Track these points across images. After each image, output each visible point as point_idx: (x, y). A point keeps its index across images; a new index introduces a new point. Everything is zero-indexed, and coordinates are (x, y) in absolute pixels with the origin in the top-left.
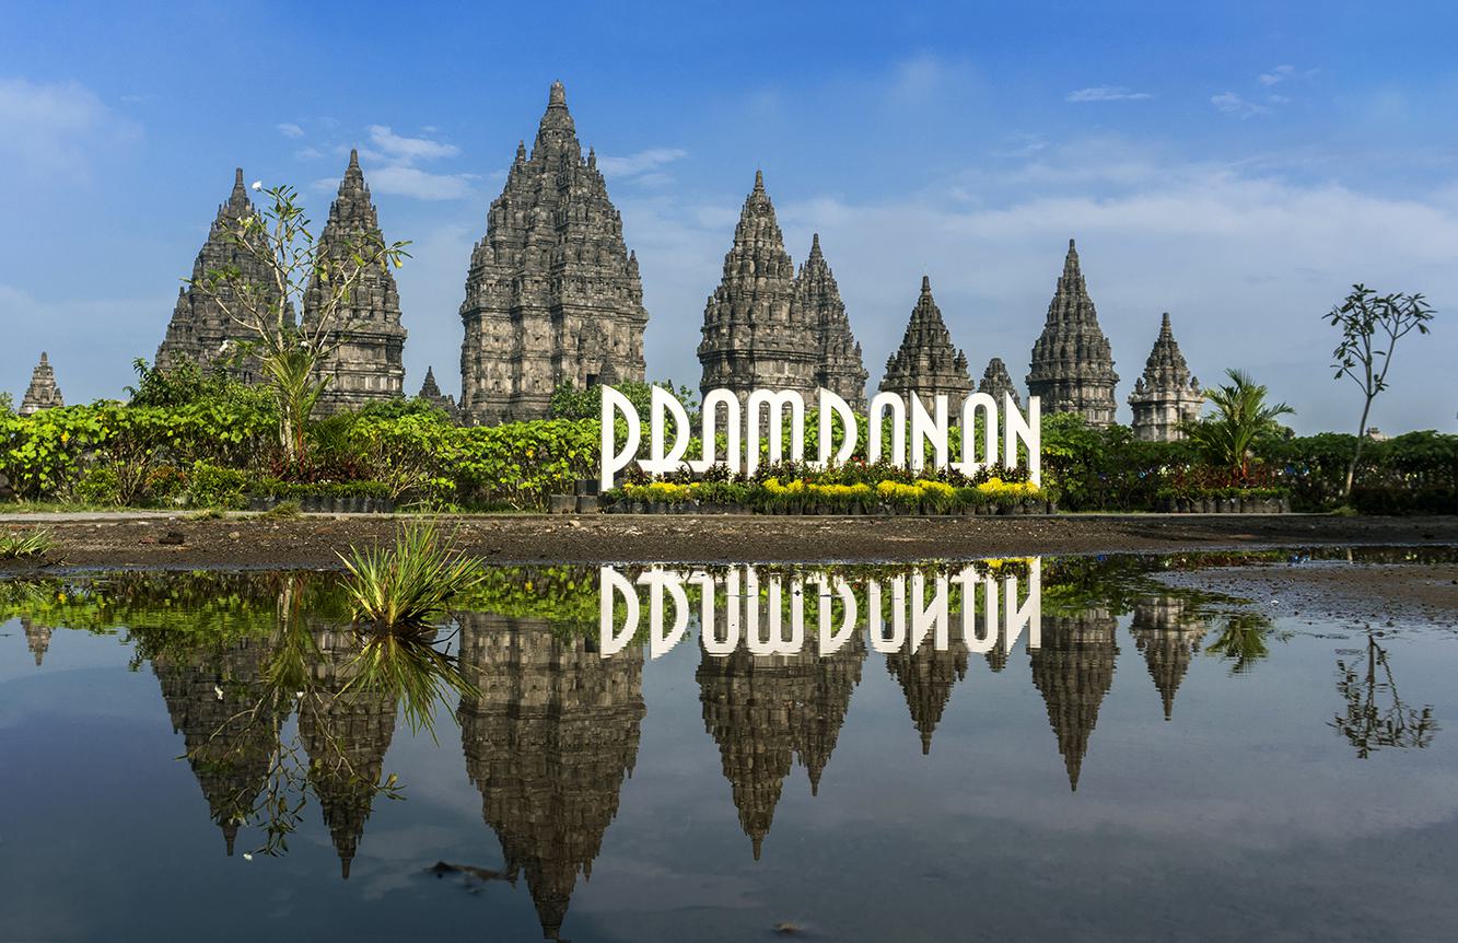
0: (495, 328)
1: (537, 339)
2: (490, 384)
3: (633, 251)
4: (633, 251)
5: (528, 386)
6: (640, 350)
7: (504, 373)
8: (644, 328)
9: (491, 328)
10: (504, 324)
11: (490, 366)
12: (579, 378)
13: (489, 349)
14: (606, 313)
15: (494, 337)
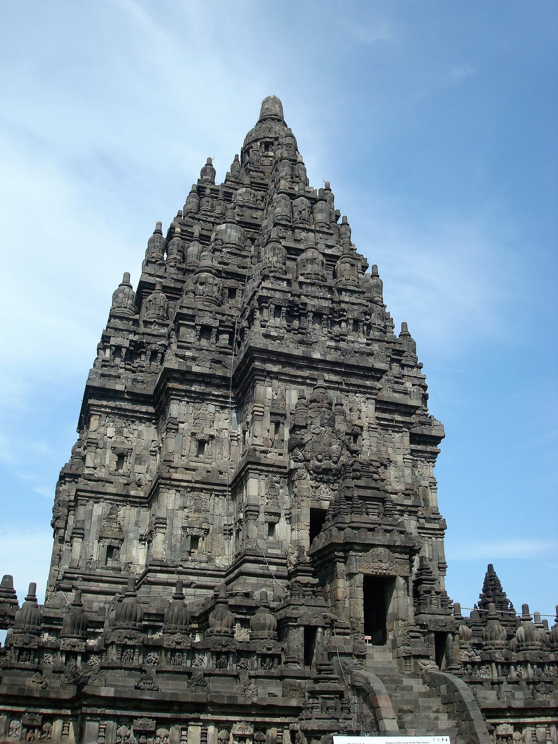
0: (119, 432)
1: (201, 444)
2: (96, 550)
3: (404, 325)
4: (404, 325)
5: (171, 548)
6: (431, 496)
7: (132, 527)
8: (435, 454)
9: (111, 431)
10: (142, 427)
11: (99, 509)
12: (289, 519)
13: (101, 473)
14: (353, 381)
15: (114, 448)
